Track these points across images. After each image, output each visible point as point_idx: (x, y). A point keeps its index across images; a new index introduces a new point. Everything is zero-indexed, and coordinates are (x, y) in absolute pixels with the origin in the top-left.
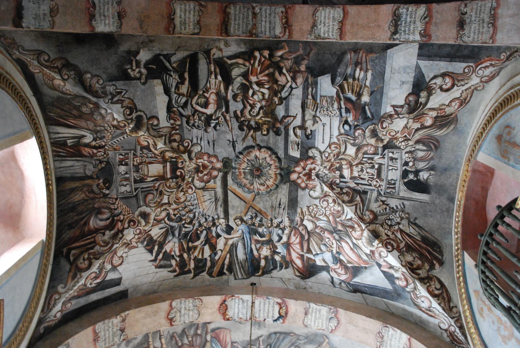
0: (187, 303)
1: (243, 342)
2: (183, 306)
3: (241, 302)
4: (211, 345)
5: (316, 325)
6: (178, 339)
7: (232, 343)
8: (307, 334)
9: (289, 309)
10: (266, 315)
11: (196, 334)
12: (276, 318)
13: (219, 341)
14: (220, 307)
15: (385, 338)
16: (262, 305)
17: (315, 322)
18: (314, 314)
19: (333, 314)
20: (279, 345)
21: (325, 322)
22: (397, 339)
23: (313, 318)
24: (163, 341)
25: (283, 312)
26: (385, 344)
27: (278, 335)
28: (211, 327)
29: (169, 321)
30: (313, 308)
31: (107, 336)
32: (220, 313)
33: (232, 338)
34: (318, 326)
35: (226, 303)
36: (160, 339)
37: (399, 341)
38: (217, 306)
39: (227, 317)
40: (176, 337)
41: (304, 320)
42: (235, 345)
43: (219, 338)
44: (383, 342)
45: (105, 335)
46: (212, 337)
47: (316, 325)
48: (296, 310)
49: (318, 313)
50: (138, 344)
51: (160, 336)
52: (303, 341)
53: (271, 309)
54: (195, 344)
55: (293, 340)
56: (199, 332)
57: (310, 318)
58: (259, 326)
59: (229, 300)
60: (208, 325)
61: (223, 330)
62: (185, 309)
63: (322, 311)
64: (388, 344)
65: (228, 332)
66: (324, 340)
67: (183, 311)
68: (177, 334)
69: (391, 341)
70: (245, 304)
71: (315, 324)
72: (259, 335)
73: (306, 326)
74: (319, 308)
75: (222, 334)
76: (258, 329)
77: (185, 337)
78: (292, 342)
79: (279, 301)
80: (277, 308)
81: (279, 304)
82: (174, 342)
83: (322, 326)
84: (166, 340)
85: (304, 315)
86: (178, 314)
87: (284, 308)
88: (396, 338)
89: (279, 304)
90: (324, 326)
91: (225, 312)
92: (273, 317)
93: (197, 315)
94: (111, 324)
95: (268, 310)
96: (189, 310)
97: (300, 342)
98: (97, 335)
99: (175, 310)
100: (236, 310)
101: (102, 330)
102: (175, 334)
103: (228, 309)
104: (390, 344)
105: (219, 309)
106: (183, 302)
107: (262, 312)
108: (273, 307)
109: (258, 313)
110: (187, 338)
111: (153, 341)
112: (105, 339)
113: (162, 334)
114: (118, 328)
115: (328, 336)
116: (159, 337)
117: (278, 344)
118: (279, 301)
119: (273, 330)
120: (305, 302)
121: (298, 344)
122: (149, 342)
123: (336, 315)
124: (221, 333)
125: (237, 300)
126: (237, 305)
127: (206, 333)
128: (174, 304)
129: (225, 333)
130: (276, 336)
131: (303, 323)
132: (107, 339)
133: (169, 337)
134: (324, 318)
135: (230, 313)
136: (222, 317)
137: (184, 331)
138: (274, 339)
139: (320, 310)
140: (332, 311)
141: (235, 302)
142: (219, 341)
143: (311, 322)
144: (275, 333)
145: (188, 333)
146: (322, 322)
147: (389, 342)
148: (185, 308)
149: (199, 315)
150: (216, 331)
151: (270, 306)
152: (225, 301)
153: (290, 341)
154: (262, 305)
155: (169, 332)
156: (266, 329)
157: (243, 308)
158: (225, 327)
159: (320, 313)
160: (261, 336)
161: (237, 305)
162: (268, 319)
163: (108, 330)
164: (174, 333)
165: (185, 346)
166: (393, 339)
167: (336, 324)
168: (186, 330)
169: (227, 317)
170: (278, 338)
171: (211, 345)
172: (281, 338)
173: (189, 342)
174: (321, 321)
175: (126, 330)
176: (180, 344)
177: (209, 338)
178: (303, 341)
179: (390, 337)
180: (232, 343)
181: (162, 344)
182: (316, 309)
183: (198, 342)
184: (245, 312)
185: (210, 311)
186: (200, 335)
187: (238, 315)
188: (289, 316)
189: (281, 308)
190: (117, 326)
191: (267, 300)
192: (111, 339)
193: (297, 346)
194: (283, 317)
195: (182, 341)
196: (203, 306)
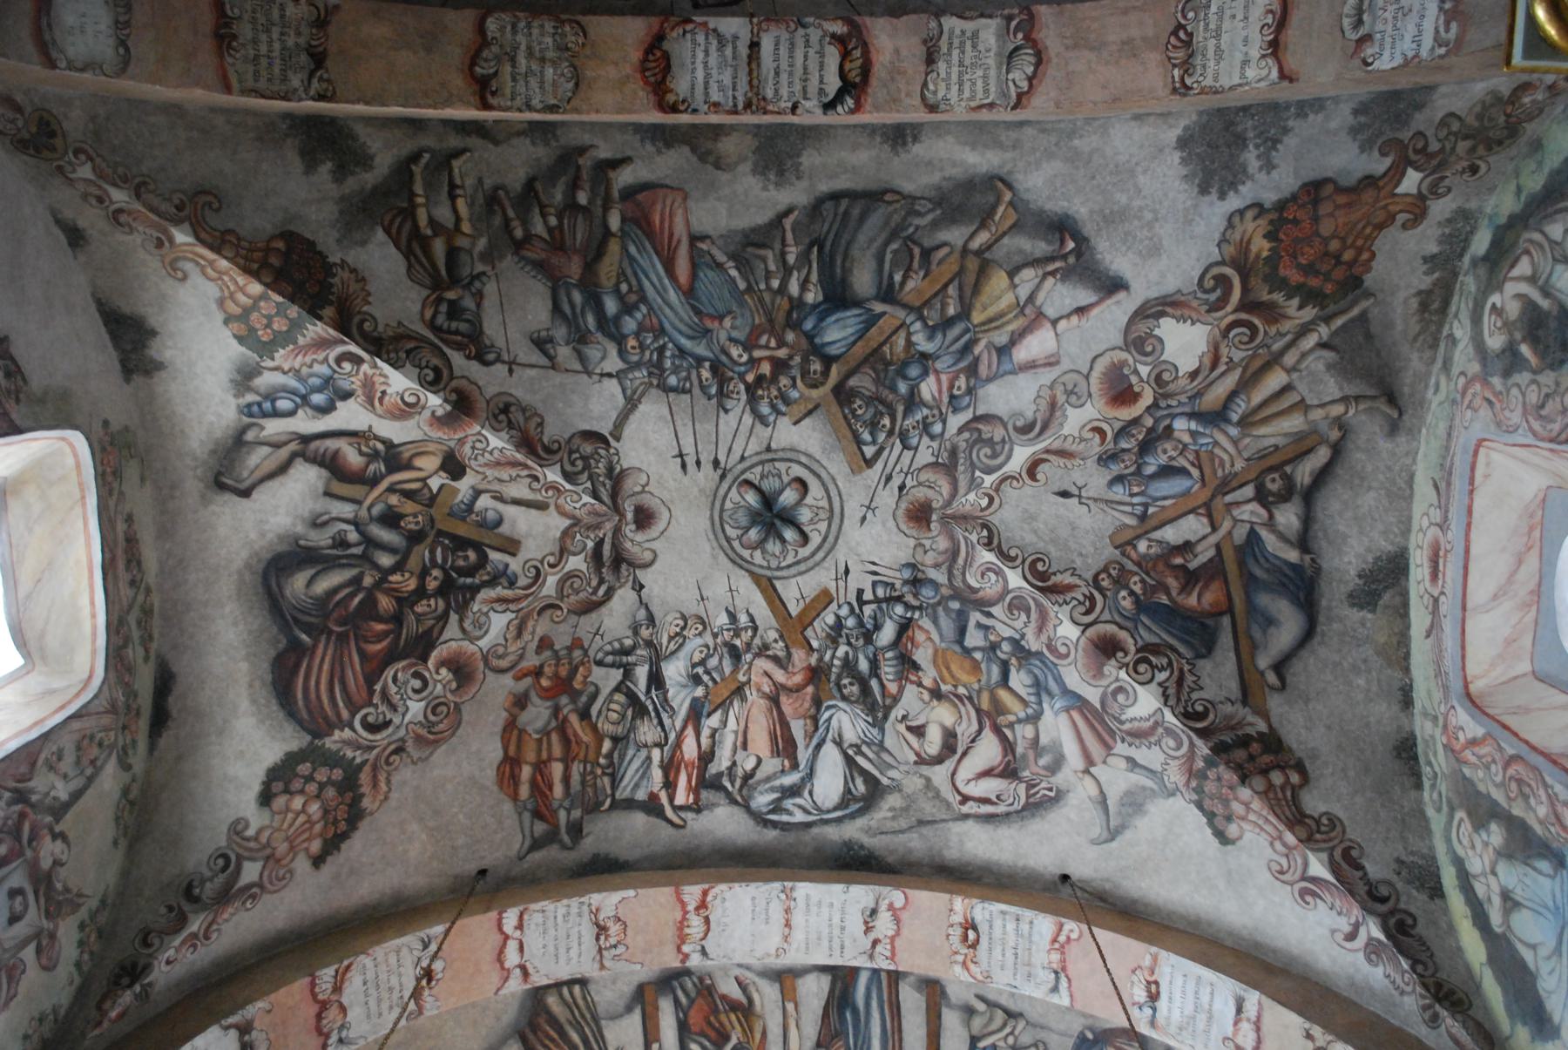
0: (535, 31)
1: (727, 236)
2: (521, 39)
3: (715, 42)
4: (625, 249)
5: (967, 94)
6: (511, 213)
7: (694, 239)
8: (939, 188)
9: (874, 56)
10: (798, 87)
11: (572, 206)
12: (831, 96)
13: (650, 234)
14: (645, 60)
15: (1199, 37)
16: (783, 51)
17: (961, 83)
18: (956, 53)
19: (1020, 36)
20: (849, 244)
21: (993, 73)
22: (1240, 16)
23: (955, 70)
24: (461, 203)
25: (853, 68)
26: (1198, 60)
27: (844, 203)
28: (625, 177)
29: (476, 88)
30: (951, 32)
31: (264, 49)
32: (647, 83)
33: (693, 220)
34: (972, 98)
35: (666, 45)
36: (453, 198)
37: (1246, 18)
38: (635, 55)
39: (671, 98)
40: (507, 203)
41: (925, 85)
42: (704, 246)
43: (649, 223)
44: (1190, 56)
45: (255, 41)
46: (624, 220)
47: (967, 94)
48: (897, 51)
49: (969, 43)
50: (375, 188)
51: (452, 186)
52: (930, 217)
53: (813, 65)
54: (568, 242)
55: (896, 218)
56: (582, 198)
57: (943, 75)
58: (781, 173)
59: (674, 34)
60: (612, 174)
61: (661, 193)
62: (530, 54)
63: (982, 35)
64: (1211, 53)
65: (679, 200)
66: (998, 200)
67: (522, 61)
68: (507, 193)
69: (1218, 36)
70: (728, 51)
71: (961, 91)
72: (781, 208)
73: (933, 108)
74: (969, 26)
75: (659, 207)
76: (777, 185)
77: (537, 210)
78: (893, 224)
79: (839, 28)
80: (833, 56)
81: (838, 39)
82: (497, 221)
83: (986, 91)
84: (471, 205)
85: (923, 68)
86: (508, 68)
87: (857, 53)
88: (1234, 17)
89: (838, 39)
90: (993, 89)
91: (664, 78)
92: (821, 92)
93: (571, 85)
94: (276, 13)
95: (805, 68)
96: (543, 60)
97: (918, 221)
98: (227, 25)
99: (495, 49)
100: (700, 74)
101: (246, 17)
102: (501, 192)
103: (674, 69)
104: (1218, 48)
105: (643, 68)
106: (522, 24)
107: (784, 77)
108: (821, 54)
109: (771, 82)
110: (544, 215)
111: (427, 198)
112: (256, 57)
113: (458, 181)
114: (302, 41)
115: (1008, 179)
116: (446, 189)
117: (846, 237)
118: (839, 28)
119: (824, 187)
120: (924, 16)
121: (911, 230)
122: (412, 195)
123: (1027, 38)
124: (654, 203)
125: (701, 38)
126: (700, 55)
127: (606, 208)
128: (492, 25)
129: (668, 202)
130: (837, 207)
131: (923, 98)
132: (264, 61)
133: (480, 200)
134: (991, 62)
135: (680, 85)
136: (652, 98)
137: (530, 184)
138: (830, 219)
139: (975, 35)
140: (1014, 23)
141: (694, 42)
142: (650, 234)
143: (948, 88)
144: (835, 196)
145: (543, 198)
146: (985, 77)
147: (1212, 43)
148: (529, 48)
149: (577, 85)
150: (640, 197)
151: (811, 52)
152: (660, 38)
153: (887, 223)
154: (783, 51)
155: (480, 181)
156: (804, 184)
157: (722, 65)
158: (668, 182)
159: (974, 46)
160: (788, 212)
161: (700, 55)
162: (808, 104)
163: (268, 31)
164: (496, 188)
165: (536, 242)
166: (1226, 25)
167: (1030, 70)
168: (538, 186)
169: (671, 98)
170: (846, 213)
171: (625, 249)
172: (856, 212)
173: (550, 230)
174: (980, 73)
175: (329, 63)
176: (519, 233)
177: (614, 222)
178: (930, 217)
179: (1212, 26)
180: (694, 239)
181: (458, 219)
182: (963, 32)
183: (579, 236)
184: (727, 79)
185: (612, 72)
186: (585, 210)
187: (707, 94)
188: (874, 81)
189: (845, 55)
190: (298, 34)
191: (801, 31)
192: (277, 70)
193: (910, 238)
194: (854, 85)
195: (525, 223)
196: (588, 51)
